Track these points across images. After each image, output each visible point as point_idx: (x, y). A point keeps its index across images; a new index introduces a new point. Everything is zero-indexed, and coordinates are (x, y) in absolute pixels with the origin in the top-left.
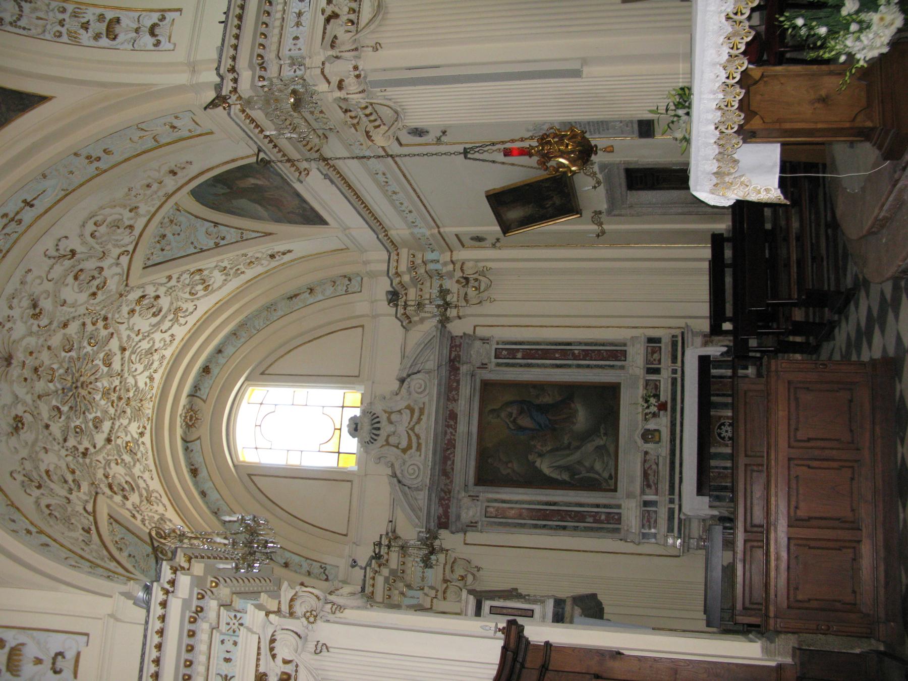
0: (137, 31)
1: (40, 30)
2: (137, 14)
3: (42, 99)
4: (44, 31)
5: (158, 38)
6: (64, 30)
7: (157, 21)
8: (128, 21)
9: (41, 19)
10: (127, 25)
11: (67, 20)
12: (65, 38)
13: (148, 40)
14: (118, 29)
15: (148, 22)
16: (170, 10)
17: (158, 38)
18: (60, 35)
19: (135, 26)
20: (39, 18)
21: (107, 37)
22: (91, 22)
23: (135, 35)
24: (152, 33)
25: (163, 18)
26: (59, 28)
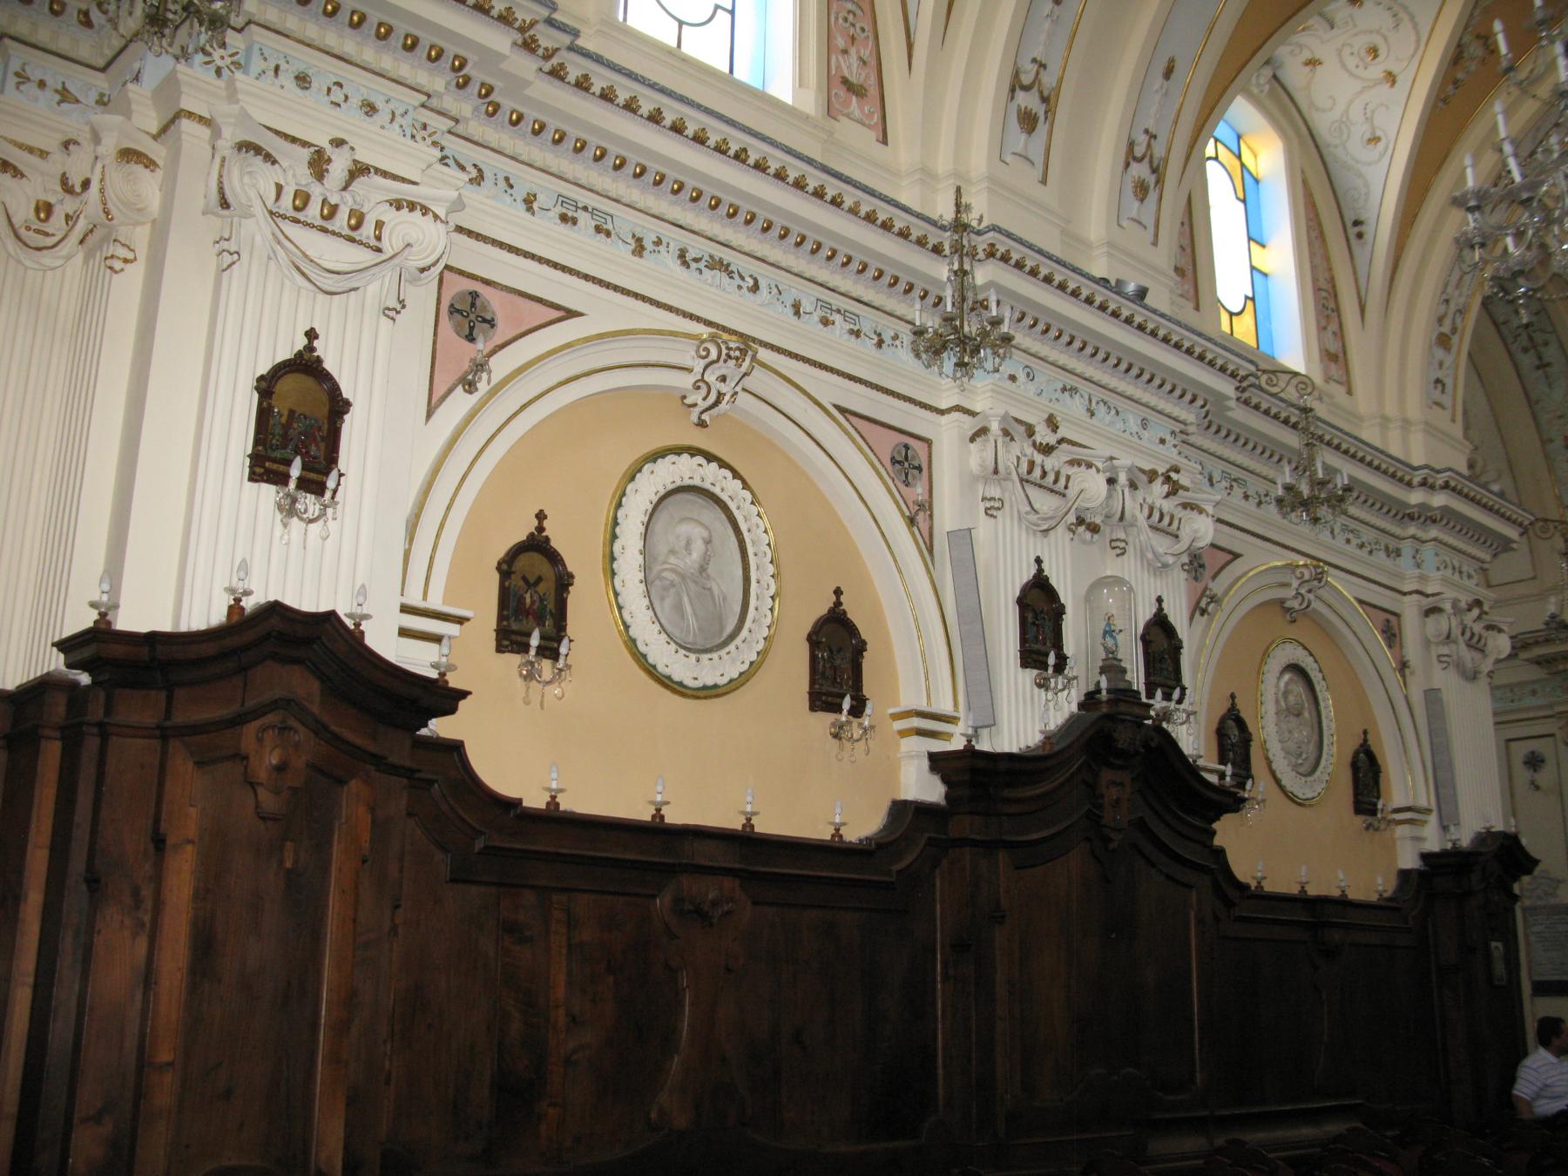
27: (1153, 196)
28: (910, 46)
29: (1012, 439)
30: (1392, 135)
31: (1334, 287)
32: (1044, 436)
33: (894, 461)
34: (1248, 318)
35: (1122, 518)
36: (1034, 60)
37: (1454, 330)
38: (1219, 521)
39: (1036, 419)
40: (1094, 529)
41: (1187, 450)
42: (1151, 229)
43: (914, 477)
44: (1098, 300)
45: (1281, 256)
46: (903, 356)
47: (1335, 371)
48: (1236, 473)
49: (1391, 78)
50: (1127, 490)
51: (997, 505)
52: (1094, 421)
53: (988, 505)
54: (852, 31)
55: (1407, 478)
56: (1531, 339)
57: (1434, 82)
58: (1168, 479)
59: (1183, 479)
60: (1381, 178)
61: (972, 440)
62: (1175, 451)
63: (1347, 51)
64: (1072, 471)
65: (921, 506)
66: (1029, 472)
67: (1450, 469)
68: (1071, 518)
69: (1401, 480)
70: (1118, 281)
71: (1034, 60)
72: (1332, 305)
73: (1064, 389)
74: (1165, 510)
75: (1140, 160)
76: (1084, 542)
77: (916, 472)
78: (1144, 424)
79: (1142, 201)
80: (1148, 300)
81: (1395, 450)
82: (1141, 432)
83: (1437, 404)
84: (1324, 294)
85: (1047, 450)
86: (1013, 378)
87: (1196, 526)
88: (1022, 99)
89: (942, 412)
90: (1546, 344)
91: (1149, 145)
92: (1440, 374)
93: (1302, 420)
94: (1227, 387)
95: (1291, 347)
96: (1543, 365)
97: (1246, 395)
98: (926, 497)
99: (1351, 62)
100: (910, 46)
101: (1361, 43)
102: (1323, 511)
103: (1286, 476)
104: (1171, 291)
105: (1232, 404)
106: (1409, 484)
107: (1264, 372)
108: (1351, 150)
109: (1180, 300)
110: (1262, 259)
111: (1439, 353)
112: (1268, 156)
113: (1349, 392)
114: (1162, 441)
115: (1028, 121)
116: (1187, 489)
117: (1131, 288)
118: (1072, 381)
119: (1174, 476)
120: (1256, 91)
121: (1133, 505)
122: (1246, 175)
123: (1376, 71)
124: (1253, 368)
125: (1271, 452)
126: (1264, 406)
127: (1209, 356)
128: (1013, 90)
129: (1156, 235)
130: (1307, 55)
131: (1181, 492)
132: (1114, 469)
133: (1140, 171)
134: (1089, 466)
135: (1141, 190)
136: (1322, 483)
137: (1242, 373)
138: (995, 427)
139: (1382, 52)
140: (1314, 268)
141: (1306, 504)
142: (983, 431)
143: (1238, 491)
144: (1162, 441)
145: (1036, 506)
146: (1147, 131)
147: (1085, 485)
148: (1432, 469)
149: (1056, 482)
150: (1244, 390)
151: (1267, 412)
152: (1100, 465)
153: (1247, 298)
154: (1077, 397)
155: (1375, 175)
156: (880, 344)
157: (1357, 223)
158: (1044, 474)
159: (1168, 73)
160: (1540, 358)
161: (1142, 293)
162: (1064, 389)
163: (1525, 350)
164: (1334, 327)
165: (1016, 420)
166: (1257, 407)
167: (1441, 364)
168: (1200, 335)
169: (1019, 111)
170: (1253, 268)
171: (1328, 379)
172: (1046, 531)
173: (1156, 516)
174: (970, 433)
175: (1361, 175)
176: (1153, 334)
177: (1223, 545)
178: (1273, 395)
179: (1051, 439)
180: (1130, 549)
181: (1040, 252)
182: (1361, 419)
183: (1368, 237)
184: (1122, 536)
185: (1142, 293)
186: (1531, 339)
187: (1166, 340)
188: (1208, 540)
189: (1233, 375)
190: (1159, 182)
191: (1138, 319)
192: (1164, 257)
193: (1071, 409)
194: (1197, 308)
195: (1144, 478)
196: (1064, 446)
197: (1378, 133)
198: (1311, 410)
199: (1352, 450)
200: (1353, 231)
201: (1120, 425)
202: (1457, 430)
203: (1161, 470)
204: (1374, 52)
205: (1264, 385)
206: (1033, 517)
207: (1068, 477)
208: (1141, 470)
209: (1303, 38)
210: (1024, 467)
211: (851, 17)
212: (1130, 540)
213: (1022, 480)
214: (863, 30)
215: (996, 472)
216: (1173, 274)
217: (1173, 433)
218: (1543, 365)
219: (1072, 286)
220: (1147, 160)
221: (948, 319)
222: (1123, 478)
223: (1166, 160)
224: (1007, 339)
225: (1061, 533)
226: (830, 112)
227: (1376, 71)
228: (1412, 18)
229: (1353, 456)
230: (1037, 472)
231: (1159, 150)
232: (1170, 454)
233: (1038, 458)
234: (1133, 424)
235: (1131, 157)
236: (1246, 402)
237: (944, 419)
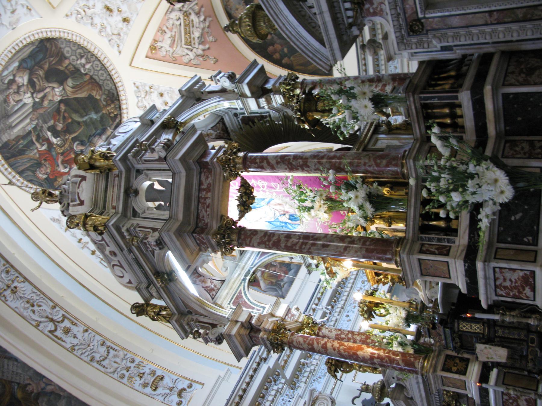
0: (171, 389)
1: (112, 370)
2: (175, 377)
4: (115, 372)
5: (182, 399)
6: (127, 374)
7: (185, 387)
8: (167, 381)
9: (117, 363)
10: (167, 383)
11: (132, 368)
12: (125, 380)
13: (175, 398)
14: (160, 384)
15: (180, 386)
16: (197, 382)
17: (182, 399)
18: (123, 377)
19: (171, 385)
20: (115, 362)
21: (151, 387)
22: (146, 374)
23: (168, 391)
24: (180, 395)
25: (190, 386)
26: (124, 372)
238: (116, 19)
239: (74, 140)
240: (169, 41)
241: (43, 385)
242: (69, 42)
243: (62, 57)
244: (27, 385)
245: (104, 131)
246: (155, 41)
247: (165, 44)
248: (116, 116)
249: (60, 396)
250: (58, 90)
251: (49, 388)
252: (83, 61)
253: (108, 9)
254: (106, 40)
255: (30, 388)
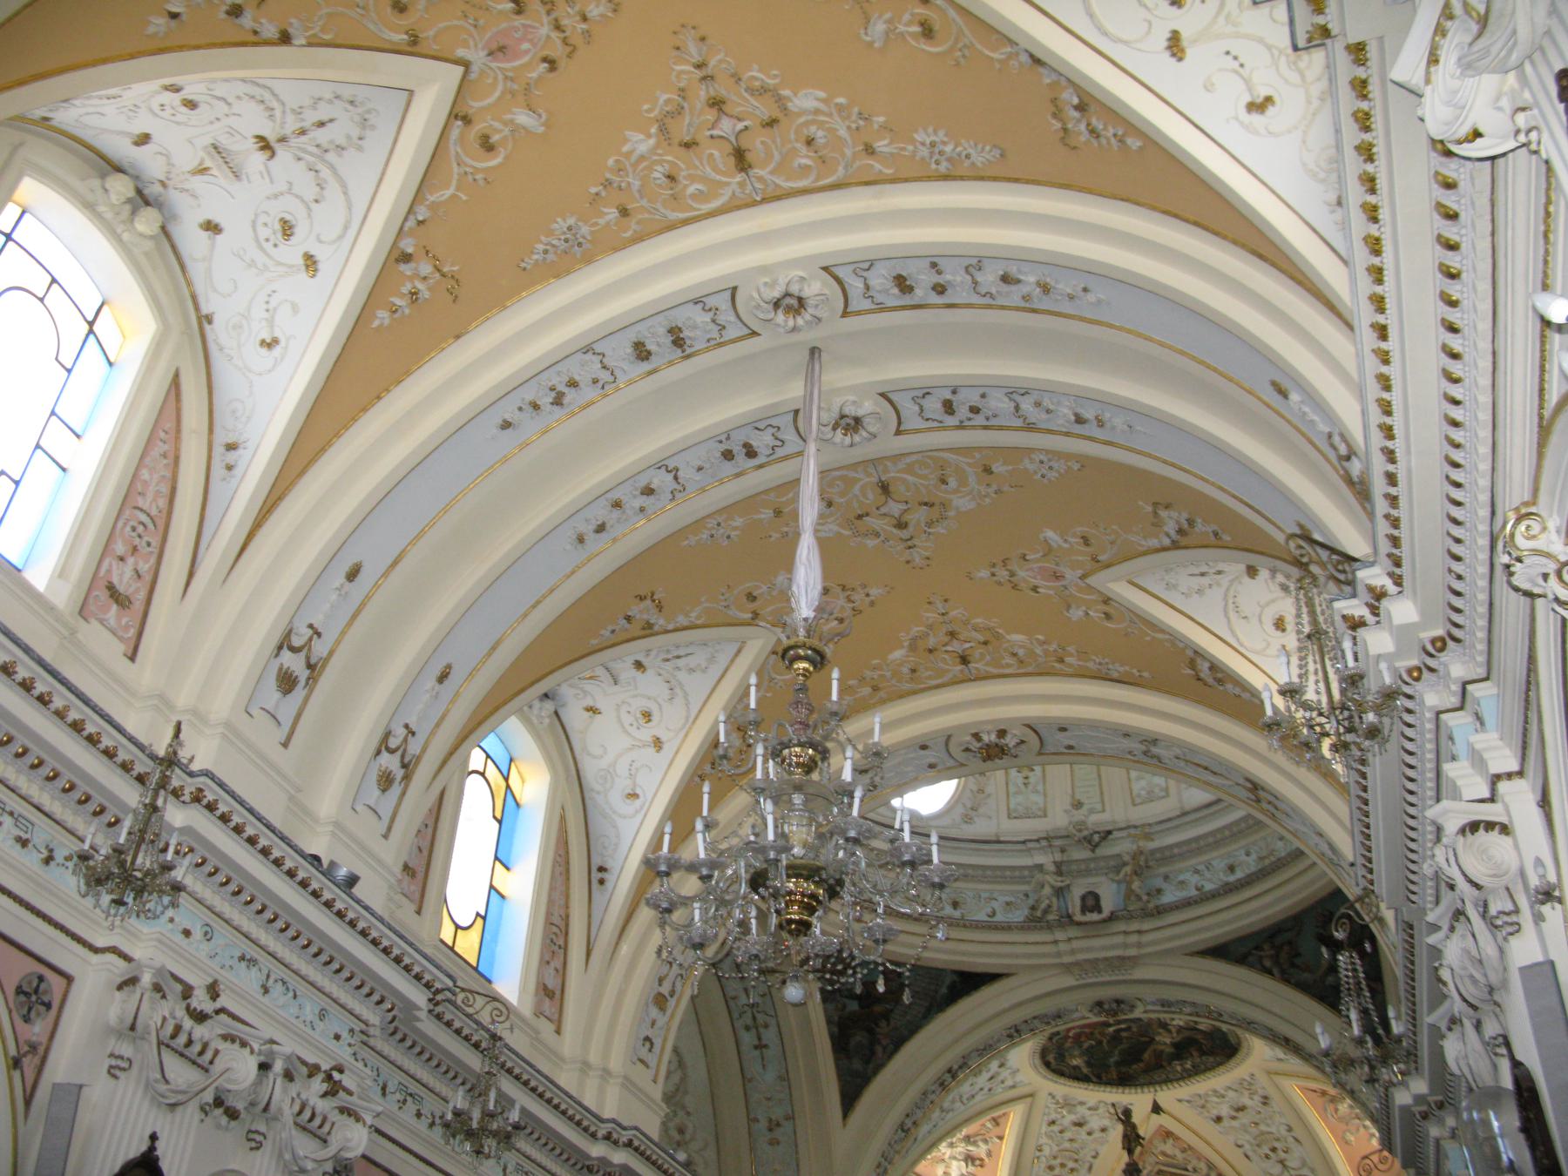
3: (845, 1115)
27: (396, 790)
28: (191, 575)
29: (164, 997)
30: (649, 796)
31: (567, 925)
32: (201, 1001)
33: (19, 991)
34: (474, 936)
35: (266, 1109)
36: (311, 626)
37: (672, 993)
38: (378, 1131)
39: (198, 981)
40: (232, 1114)
41: (365, 1053)
42: (386, 820)
43: (38, 1014)
44: (301, 875)
45: (522, 884)
46: (69, 881)
47: (547, 1004)
48: (414, 1087)
49: (658, 743)
50: (279, 1081)
51: (125, 1065)
52: (266, 1000)
53: (114, 1062)
54: (137, 541)
55: (593, 1129)
56: (754, 1018)
57: (693, 759)
58: (329, 1077)
59: (347, 1080)
60: (634, 833)
61: (120, 988)
62: (350, 1050)
63: (624, 708)
64: (223, 1046)
65: (33, 1048)
66: (173, 1037)
67: (636, 1128)
68: (209, 1097)
69: (586, 1130)
70: (332, 864)
71: (311, 626)
72: (561, 942)
73: (242, 958)
74: (318, 1111)
75: (392, 751)
76: (219, 1126)
77: (42, 1009)
78: (322, 1015)
79: (384, 791)
80: (356, 890)
81: (589, 1101)
82: (317, 1021)
83: (642, 1061)
84: (555, 929)
85: (200, 1017)
86: (187, 933)
87: (349, 1135)
88: (289, 660)
89: (96, 950)
90: (766, 1026)
91: (405, 740)
92: (649, 1033)
93: (490, 1044)
94: (419, 997)
95: (510, 979)
96: (760, 1046)
97: (439, 1009)
98: (44, 1040)
99: (627, 719)
100: (191, 575)
101: (641, 704)
102: (490, 1144)
103: (459, 1100)
104: (391, 887)
105: (423, 1015)
106: (593, 1135)
107: (463, 990)
108: (611, 799)
109: (399, 897)
110: (503, 880)
111: (654, 1012)
112: (534, 785)
113: (558, 1032)
114: (337, 1037)
115: (287, 682)
116: (350, 1093)
117: (342, 872)
118: (252, 951)
119: (336, 1075)
120: (535, 721)
121: (282, 1096)
122: (509, 796)
123: (646, 734)
124: (450, 984)
125: (452, 1071)
126: (457, 1024)
127: (407, 960)
128: (280, 648)
129: (389, 829)
130: (589, 702)
131: (342, 1094)
132: (271, 1053)
133: (390, 762)
134: (244, 1044)
135: (386, 781)
136: (492, 1115)
137: (438, 985)
138: (147, 979)
139: (656, 717)
140: (551, 902)
141: (470, 1134)
142: (132, 981)
143: (411, 1107)
144: (337, 1037)
145: (170, 1075)
146: (406, 726)
147: (234, 1065)
148: (619, 1125)
149: (201, 1053)
150: (437, 1004)
151: (458, 1032)
152: (256, 1047)
153: (478, 914)
154: (254, 970)
155: (627, 828)
156: (48, 860)
157: (601, 869)
158: (190, 1043)
159: (443, 678)
160: (760, 1039)
161: (352, 880)
162: (242, 958)
163: (747, 1028)
164: (557, 963)
165: (172, 975)
166: (449, 1024)
167: (653, 1024)
168: (402, 937)
169: (280, 669)
170: (492, 887)
171: (538, 1013)
172: (173, 1106)
173: (307, 1114)
174: (119, 980)
175: (615, 827)
176: (352, 924)
177: (378, 1159)
178: (469, 1016)
179: (208, 1006)
180: (268, 1145)
181: (251, 811)
182: (563, 1060)
183: (609, 885)
184: (262, 1128)
185: (352, 880)
186: (754, 1018)
187: (364, 933)
188: (359, 1152)
189: (428, 986)
190: (407, 778)
191: (339, 905)
192: (393, 853)
193: (249, 980)
194: (419, 912)
195: (305, 1070)
196: (223, 1016)
197: (638, 791)
198: (500, 1039)
199: (541, 1089)
200: (596, 875)
201: (294, 1010)
202: (657, 1092)
203: (325, 1066)
204: (647, 716)
205: (459, 1002)
206: (163, 1087)
207: (217, 1052)
208: (304, 1063)
209: (589, 686)
210: (169, 1029)
211: (140, 529)
212: (270, 1136)
213: (160, 1043)
214: (149, 544)
215: (133, 1028)
216: (398, 869)
217: (352, 1031)
218: (760, 1046)
219: (276, 853)
220: (399, 753)
221: (118, 851)
222: (278, 1066)
223: (418, 758)
224: (177, 888)
225: (191, 1112)
226: (83, 612)
227: (646, 734)
228: (686, 695)
229: (541, 1096)
230: (182, 1039)
231: (414, 747)
232: (343, 1053)
233: (188, 1023)
234: (310, 1011)
235: (384, 746)
236: (439, 1017)
237: (95, 959)
238: (1225, 1111)
239: (1100, 1042)
240: (1169, 1152)
241: (884, 1042)
242: (1220, 1064)
243: (1203, 1053)
244: (888, 1020)
245: (1089, 1064)
246: (1177, 1138)
247: (1168, 1147)
248: (1099, 1077)
249: (867, 1062)
250: (1168, 1041)
251: (879, 1049)
252: (1188, 1065)
253: (1241, 1109)
254: (1202, 1092)
255: (883, 1024)
